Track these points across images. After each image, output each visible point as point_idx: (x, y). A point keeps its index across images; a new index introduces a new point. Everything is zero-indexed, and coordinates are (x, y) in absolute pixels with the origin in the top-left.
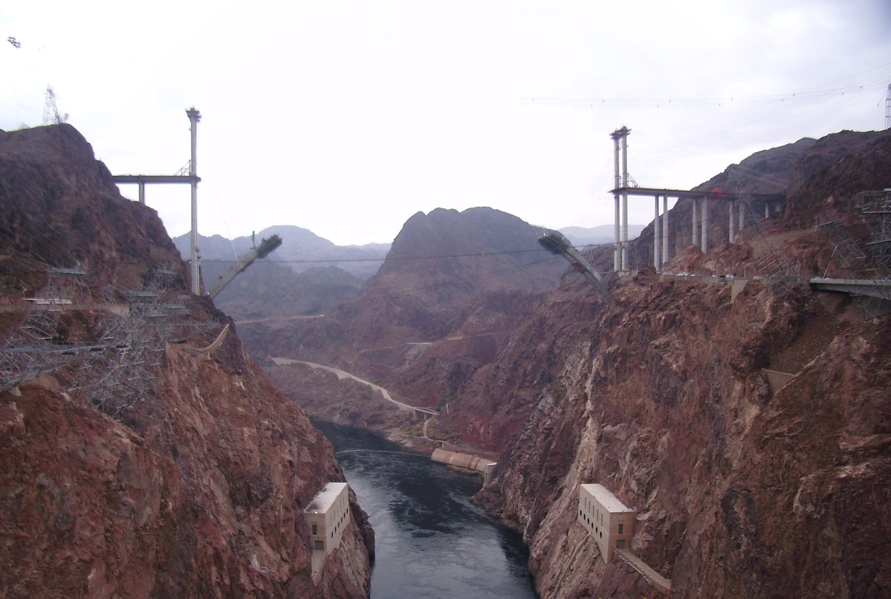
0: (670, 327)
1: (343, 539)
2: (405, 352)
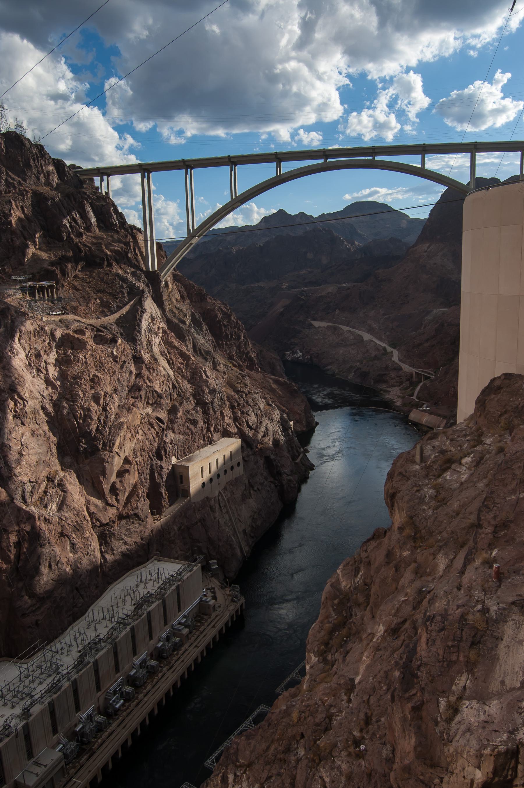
1: (225, 489)
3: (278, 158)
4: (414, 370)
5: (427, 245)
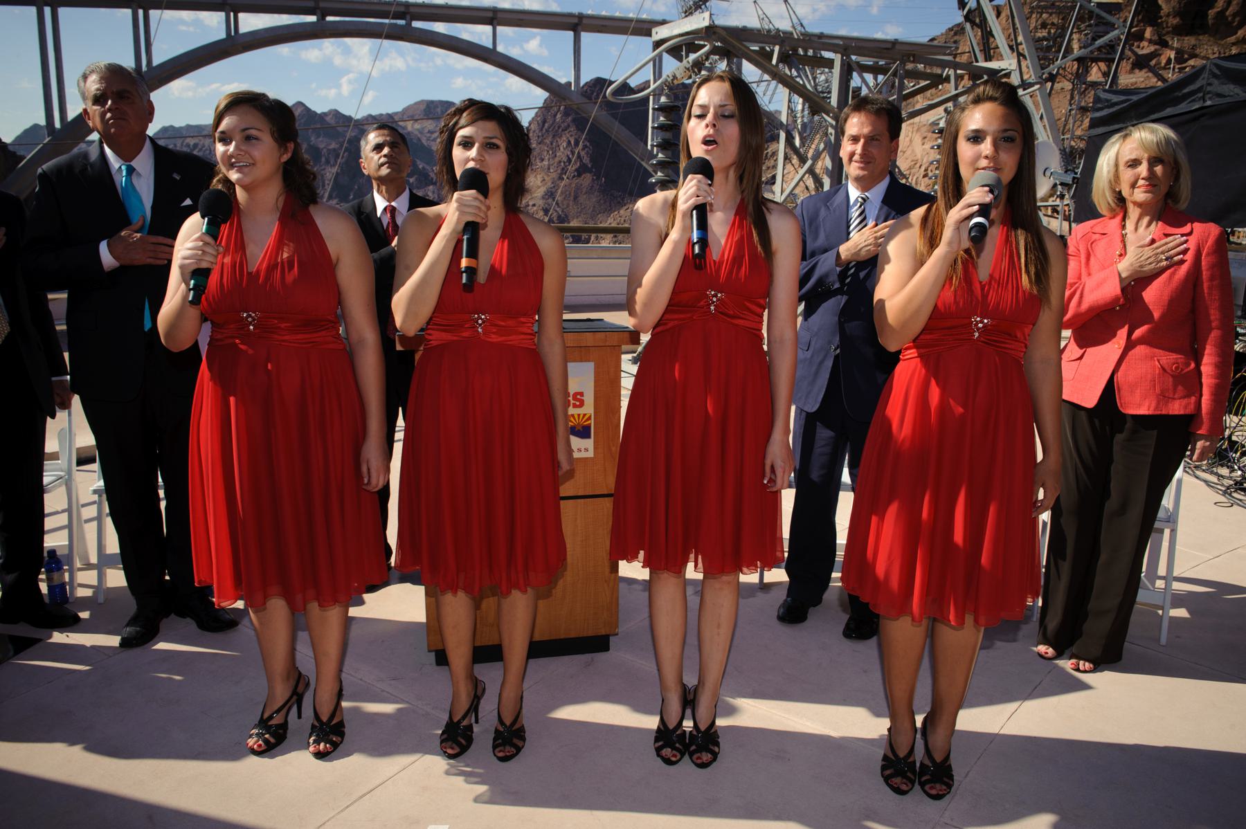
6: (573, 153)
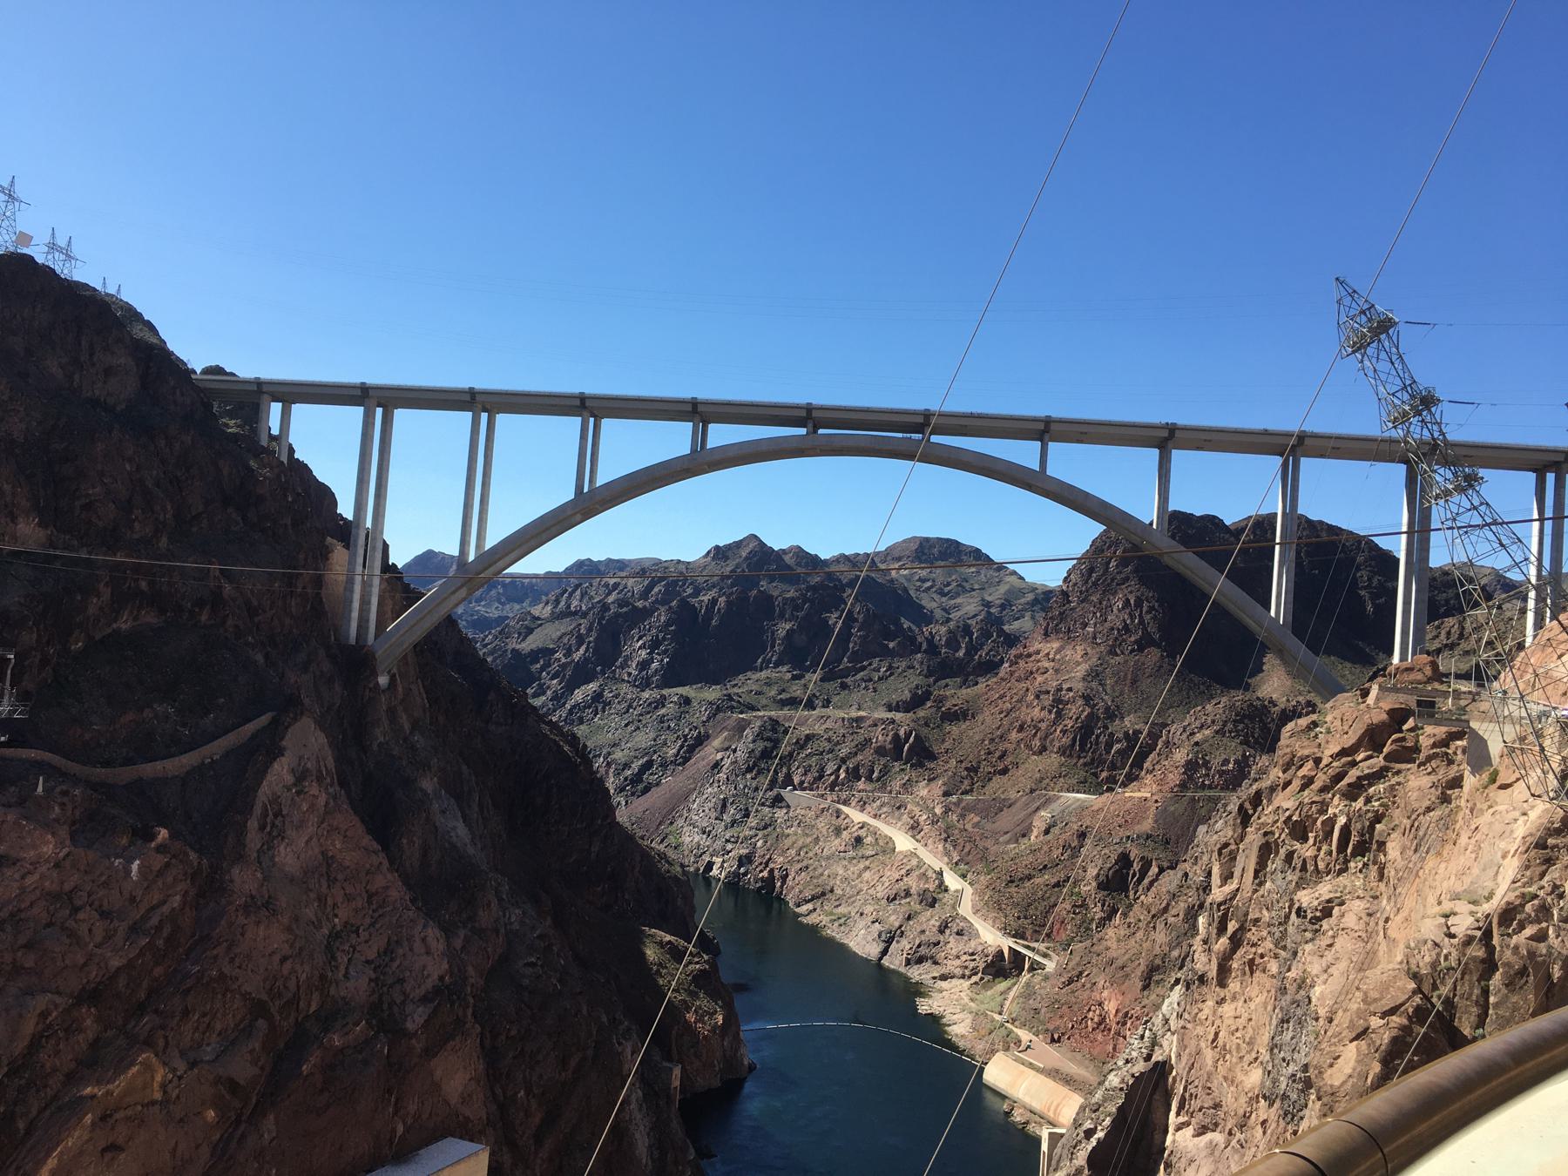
0: (1361, 849)
2: (1038, 809)
3: (698, 413)
4: (1007, 944)
5: (1056, 645)
6: (1132, 617)
